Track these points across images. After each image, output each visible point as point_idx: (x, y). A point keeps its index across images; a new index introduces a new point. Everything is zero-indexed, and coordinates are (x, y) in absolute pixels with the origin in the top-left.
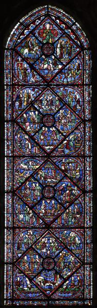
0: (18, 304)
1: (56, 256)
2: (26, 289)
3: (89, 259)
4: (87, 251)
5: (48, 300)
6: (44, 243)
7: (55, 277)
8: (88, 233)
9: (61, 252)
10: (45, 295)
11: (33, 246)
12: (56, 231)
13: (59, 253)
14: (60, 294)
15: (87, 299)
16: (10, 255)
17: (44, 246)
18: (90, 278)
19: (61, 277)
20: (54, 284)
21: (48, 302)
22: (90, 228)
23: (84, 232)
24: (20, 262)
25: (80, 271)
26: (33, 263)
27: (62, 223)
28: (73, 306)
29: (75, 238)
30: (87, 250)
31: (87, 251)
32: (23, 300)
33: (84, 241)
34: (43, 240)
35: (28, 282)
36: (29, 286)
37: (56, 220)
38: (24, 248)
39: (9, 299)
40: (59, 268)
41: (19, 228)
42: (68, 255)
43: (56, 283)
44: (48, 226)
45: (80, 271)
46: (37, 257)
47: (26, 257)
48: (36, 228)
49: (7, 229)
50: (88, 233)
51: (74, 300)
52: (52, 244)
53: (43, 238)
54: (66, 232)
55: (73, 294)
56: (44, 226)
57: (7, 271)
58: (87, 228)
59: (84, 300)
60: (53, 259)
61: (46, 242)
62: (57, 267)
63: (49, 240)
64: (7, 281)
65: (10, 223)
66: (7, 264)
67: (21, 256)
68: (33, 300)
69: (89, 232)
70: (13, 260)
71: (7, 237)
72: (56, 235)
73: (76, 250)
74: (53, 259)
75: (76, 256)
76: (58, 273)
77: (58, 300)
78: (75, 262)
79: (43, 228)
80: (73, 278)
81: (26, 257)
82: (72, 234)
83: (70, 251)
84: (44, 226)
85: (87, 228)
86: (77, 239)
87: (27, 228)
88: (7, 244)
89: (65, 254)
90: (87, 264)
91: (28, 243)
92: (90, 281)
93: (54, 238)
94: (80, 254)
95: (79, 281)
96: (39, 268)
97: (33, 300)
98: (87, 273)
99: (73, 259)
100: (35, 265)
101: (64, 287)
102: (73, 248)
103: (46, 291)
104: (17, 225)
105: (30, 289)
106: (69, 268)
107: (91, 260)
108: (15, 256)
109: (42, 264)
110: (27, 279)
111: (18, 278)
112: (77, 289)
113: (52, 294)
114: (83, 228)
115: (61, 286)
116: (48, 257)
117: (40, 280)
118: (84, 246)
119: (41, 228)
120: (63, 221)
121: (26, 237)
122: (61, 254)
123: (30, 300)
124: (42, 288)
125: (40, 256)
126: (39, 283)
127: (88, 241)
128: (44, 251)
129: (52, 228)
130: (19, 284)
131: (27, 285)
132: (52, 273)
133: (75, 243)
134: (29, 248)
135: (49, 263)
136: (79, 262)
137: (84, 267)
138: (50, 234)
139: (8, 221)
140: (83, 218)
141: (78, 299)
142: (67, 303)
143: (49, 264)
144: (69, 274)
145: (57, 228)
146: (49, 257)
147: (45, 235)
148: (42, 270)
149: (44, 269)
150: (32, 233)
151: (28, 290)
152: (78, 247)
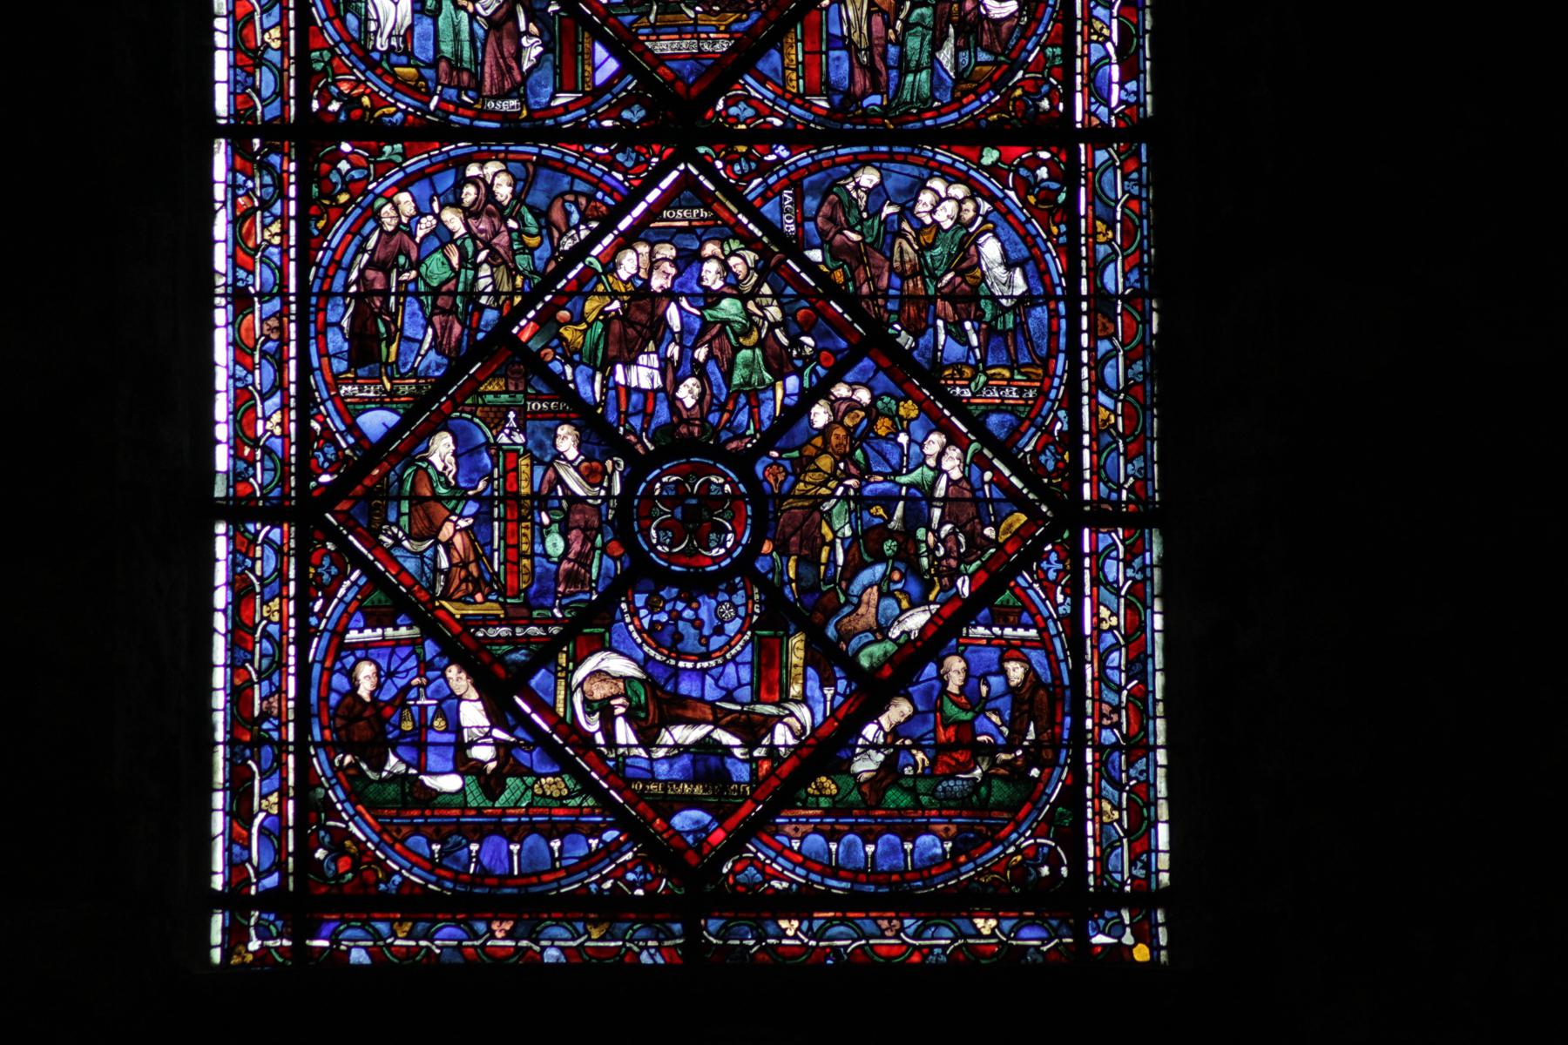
0: (359, 956)
1: (768, 439)
2: (450, 783)
3: (1124, 470)
4: (1099, 383)
5: (690, 909)
6: (641, 292)
7: (768, 661)
8: (1117, 187)
9: (820, 391)
10: (663, 853)
11: (525, 329)
12: (764, 169)
13: (807, 399)
14: (816, 841)
15: (1110, 898)
16: (271, 421)
17: (639, 322)
18: (1137, 665)
19: (828, 658)
20: (753, 729)
21: (693, 932)
22: (1127, 132)
23: (1069, 176)
24: (386, 495)
25: (1036, 593)
26: (523, 508)
27: (828, 89)
28: (967, 963)
29: (965, 242)
30: (1098, 364)
31: (1099, 383)
32: (416, 906)
33: (1072, 275)
34: (628, 264)
35: (473, 715)
36: (483, 753)
37: (761, 51)
38: (420, 346)
39: (266, 901)
40: (809, 560)
41: (370, 131)
42: (900, 424)
43: (769, 724)
44: (676, 115)
45: (1036, 593)
46: (567, 442)
47: (442, 448)
48: (556, 135)
49: (239, 148)
50: (1117, 187)
51: (955, 904)
52: (729, 307)
53: (627, 241)
54: (869, 178)
55: (966, 844)
56: (634, 115)
57: (241, 591)
58: (1099, 136)
59: (1074, 902)
60: (743, 463)
61: (658, 282)
62: (783, 549)
63: (689, 260)
64: (239, 695)
65: (266, 80)
66: (240, 511)
67: (392, 433)
68: (530, 904)
69: (1117, 181)
70: (307, 471)
71: (240, 226)
72: (769, 210)
73: (981, 367)
74: (743, 463)
75: (986, 437)
76: (800, 612)
77: (801, 903)
78: (979, 501)
79: (624, 136)
80: (955, 665)
81: (442, 448)
82: (942, 204)
83: (919, 377)
84: (634, 115)
85: (1099, 136)
86: (991, 249)
87: (446, 133)
88: (241, 300)
89: (872, 412)
90: (1103, 517)
91: (472, 295)
92: (1141, 698)
93: (750, 242)
94: (1027, 417)
95: (1024, 701)
96: (583, 560)
97: (530, 904)
98: (1103, 616)
99: (952, 464)
100: (544, 531)
101: (866, 765)
102: (955, 351)
103: (670, 805)
104: (350, 102)
105: (491, 784)
106: (907, 555)
107: (1143, 479)
108: (328, 436)
109: (626, 518)
110: (458, 679)
111: (366, 672)
112: (1000, 791)
113: (734, 846)
114: (1060, 132)
115: (828, 749)
116: (685, 442)
117: (599, 691)
118: (1074, 332)
119: (603, 137)
120: (839, 66)
121: (439, 223)
122: (820, 415)
123: (495, 907)
124: (620, 773)
125: (600, 435)
126: (592, 725)
127: (1113, 278)
128: (643, 374)
129: (724, 136)
130: (365, 729)
131: (461, 748)
132: (728, 616)
133: (969, 296)
134: (477, 351)
135: (702, 512)
136: (1021, 504)
137: (1073, 554)
138: (705, 199)
139: (248, 56)
140: (1046, 26)
141: (1014, 894)
142: (896, 936)
143: (696, 519)
144: (916, 620)
145: (771, 137)
146: (688, 446)
147: (653, 212)
148: (619, 587)
149: (639, 567)
150: (503, 191)
151: (475, 798)
152: (1006, 337)
